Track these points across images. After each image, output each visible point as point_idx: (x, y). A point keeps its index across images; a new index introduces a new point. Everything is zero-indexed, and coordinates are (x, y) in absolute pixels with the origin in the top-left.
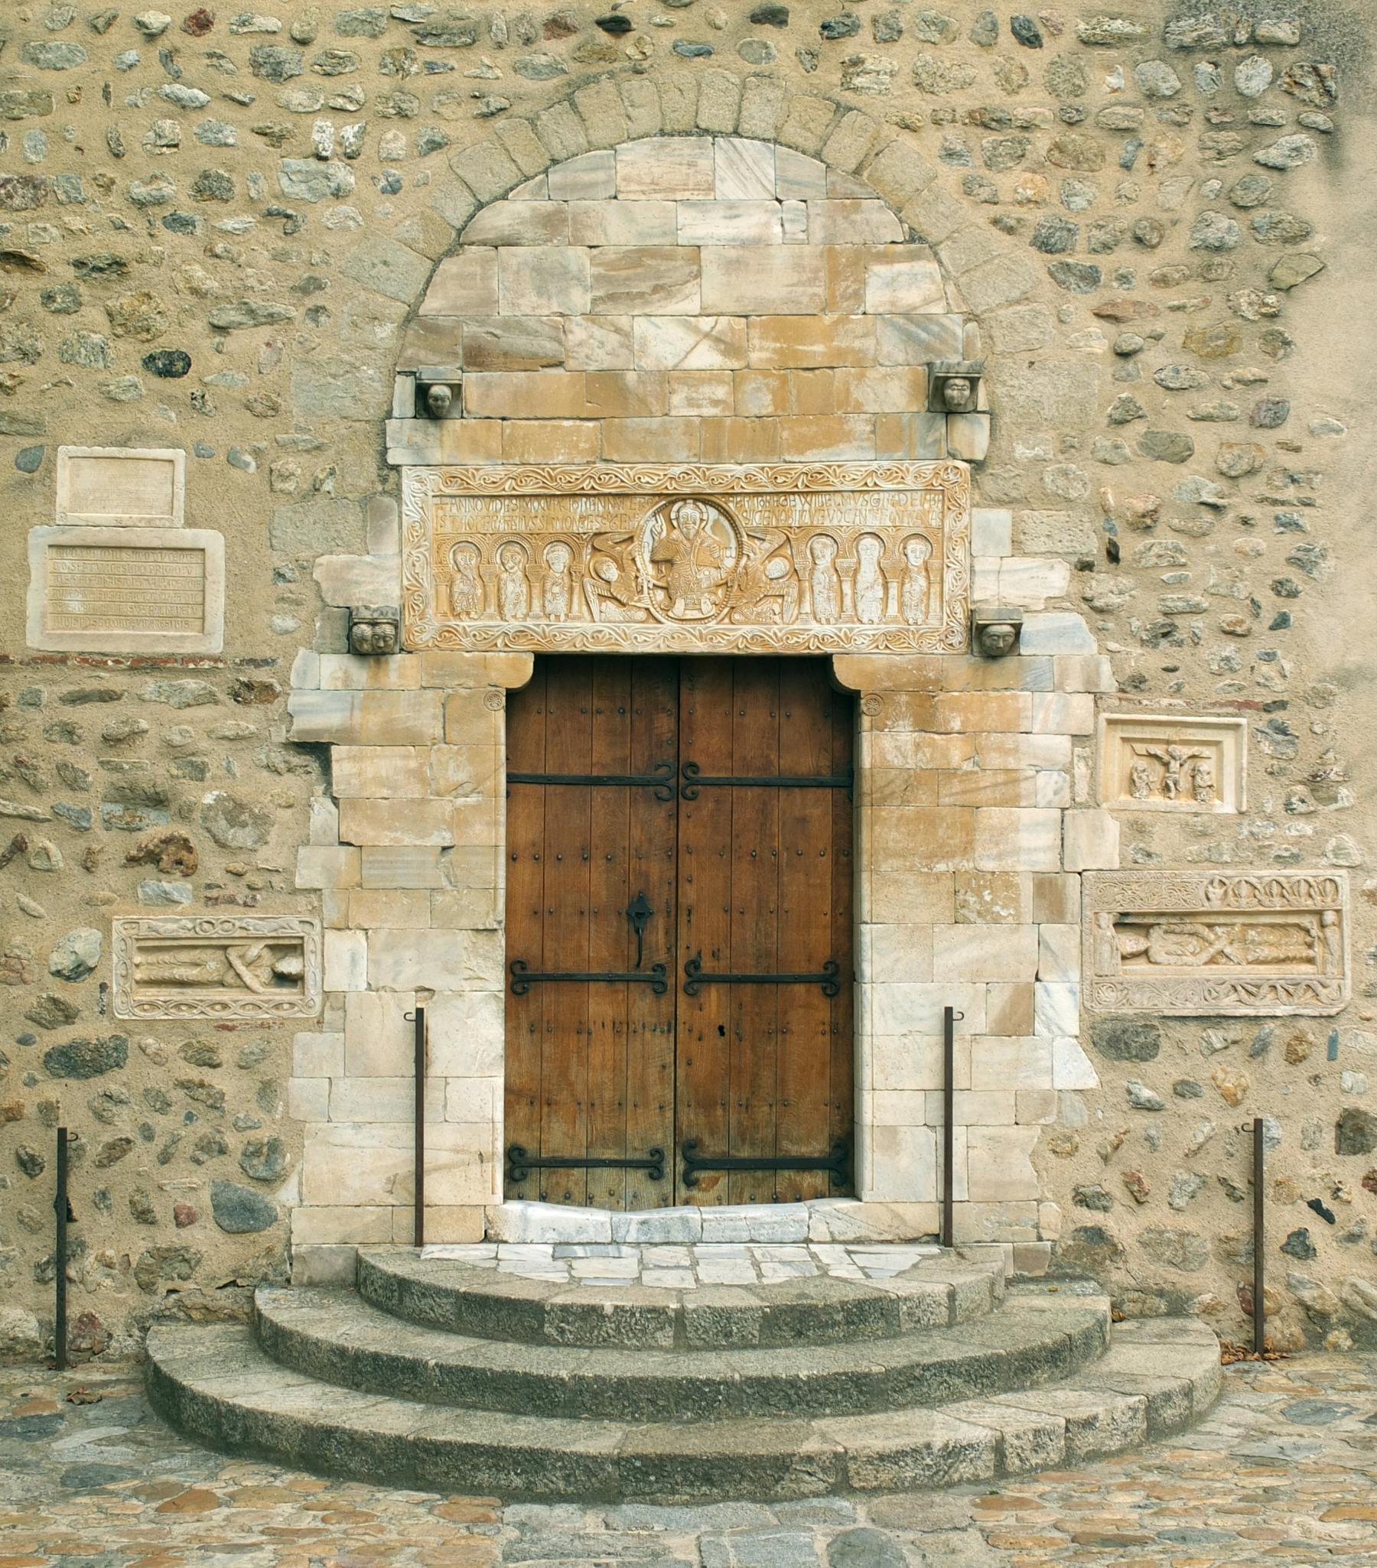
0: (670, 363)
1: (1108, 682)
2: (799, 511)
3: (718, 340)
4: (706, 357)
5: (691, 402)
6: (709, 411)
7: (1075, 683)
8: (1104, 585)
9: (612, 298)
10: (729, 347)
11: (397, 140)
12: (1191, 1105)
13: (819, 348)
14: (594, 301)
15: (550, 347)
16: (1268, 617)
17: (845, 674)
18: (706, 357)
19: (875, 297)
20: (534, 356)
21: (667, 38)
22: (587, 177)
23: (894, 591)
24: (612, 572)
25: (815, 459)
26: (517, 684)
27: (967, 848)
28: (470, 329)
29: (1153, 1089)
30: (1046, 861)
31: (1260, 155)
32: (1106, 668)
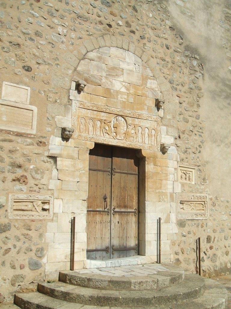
0: (118, 89)
1: (179, 160)
2: (137, 121)
3: (125, 87)
4: (123, 90)
5: (121, 98)
6: (124, 100)
7: (174, 159)
8: (179, 142)
9: (109, 75)
10: (128, 89)
11: (73, 35)
12: (190, 235)
13: (140, 92)
14: (106, 75)
15: (99, 82)
16: (198, 151)
17: (144, 153)
18: (123, 90)
19: (148, 85)
20: (96, 83)
21: (118, 31)
22: (106, 51)
23: (150, 139)
24: (107, 128)
25: (140, 112)
26: (92, 148)
27: (161, 187)
28: (86, 75)
29: (185, 233)
30: (171, 191)
31: (196, 75)
32: (178, 157)
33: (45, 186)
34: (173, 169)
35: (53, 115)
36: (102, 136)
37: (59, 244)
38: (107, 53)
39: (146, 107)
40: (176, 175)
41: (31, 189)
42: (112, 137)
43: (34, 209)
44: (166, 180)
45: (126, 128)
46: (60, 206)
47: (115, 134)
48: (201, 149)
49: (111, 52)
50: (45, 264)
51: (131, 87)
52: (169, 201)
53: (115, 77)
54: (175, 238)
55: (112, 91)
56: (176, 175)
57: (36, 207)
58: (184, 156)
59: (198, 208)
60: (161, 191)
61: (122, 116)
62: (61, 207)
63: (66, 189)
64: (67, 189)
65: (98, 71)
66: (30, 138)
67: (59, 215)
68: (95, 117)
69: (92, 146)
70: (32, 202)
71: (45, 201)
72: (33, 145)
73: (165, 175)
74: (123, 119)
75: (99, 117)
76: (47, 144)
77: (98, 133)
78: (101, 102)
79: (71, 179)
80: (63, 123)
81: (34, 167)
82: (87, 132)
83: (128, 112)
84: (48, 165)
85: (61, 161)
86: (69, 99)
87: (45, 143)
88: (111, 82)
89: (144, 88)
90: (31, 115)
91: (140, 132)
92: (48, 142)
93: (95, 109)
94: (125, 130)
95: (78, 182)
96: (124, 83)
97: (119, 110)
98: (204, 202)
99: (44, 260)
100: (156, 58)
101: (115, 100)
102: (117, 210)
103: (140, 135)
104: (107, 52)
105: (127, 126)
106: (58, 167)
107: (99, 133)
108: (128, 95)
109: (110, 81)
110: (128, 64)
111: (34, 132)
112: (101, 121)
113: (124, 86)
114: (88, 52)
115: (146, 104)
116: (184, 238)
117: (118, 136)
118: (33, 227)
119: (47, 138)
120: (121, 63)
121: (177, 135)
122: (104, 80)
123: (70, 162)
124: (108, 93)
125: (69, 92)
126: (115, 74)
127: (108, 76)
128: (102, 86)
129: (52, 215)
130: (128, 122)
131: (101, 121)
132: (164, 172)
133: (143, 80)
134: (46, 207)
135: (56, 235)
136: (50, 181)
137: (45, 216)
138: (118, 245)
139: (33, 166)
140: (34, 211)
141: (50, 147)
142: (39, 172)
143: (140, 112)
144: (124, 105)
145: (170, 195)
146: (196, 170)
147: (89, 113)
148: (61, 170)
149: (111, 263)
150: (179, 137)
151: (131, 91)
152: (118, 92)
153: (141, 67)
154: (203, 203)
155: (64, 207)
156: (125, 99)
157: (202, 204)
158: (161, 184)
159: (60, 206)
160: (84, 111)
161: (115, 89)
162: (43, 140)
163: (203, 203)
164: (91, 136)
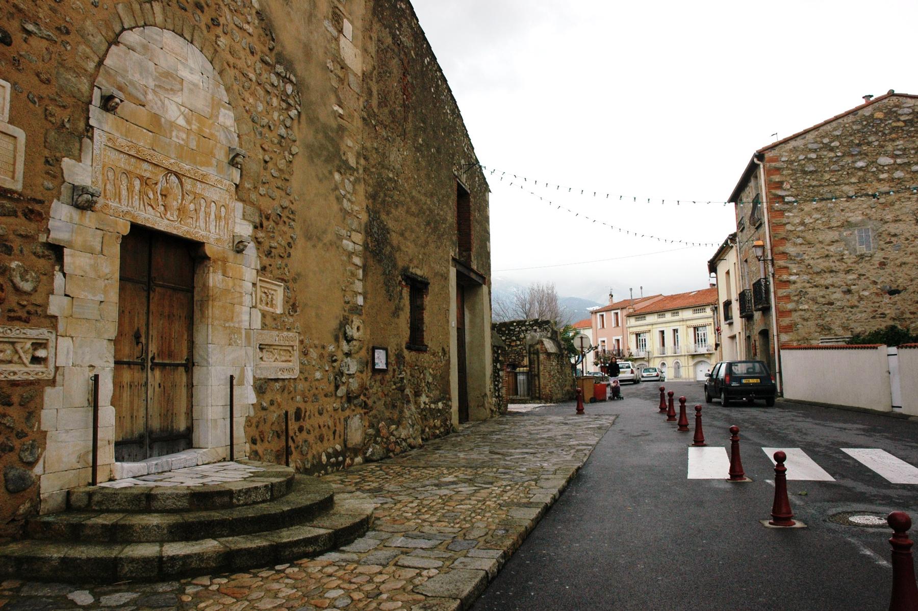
0: (173, 119)
4: (181, 122)
5: (177, 137)
6: (182, 142)
8: (260, 234)
9: (160, 86)
10: (188, 122)
12: (272, 408)
14: (155, 85)
15: (142, 97)
17: (208, 251)
18: (181, 122)
20: (138, 99)
22: (155, 37)
24: (151, 196)
26: (125, 234)
33: (39, 310)
34: (251, 285)
35: (58, 155)
36: (142, 211)
37: (67, 431)
38: (156, 40)
39: (214, 162)
40: (254, 295)
41: (12, 314)
42: (159, 215)
43: (16, 358)
44: (241, 304)
45: (180, 197)
46: (68, 353)
47: (163, 208)
48: (291, 251)
49: (165, 40)
50: (40, 477)
51: (194, 118)
52: (244, 345)
53: (169, 94)
54: (252, 414)
55: (163, 120)
56: (254, 295)
57: (22, 354)
58: (266, 261)
59: (284, 358)
60: (232, 325)
61: (176, 174)
62: (71, 353)
63: (79, 316)
64: (82, 317)
65: (141, 74)
66: (11, 199)
67: (67, 371)
68: (131, 168)
69: (126, 230)
70: (13, 343)
71: (38, 341)
72: (17, 216)
73: (239, 295)
74: (177, 181)
75: (138, 172)
76: (44, 216)
77: (136, 204)
78: (144, 141)
79: (90, 297)
80: (77, 174)
81: (18, 266)
82: (117, 200)
83: (188, 167)
84: (42, 263)
85: (72, 255)
86: (87, 124)
87: (40, 214)
88: (163, 103)
89: (213, 124)
90: (11, 147)
91: (203, 209)
92: (48, 213)
93: (132, 153)
94: (180, 201)
95: (101, 302)
96: (183, 109)
97: (172, 161)
98: (292, 346)
99: (38, 469)
100: (234, 67)
101: (168, 140)
102: (156, 361)
103: (202, 215)
104: (158, 38)
105: (183, 195)
106: (67, 269)
107: (138, 202)
108: (189, 131)
109: (161, 100)
110: (192, 71)
111: (18, 187)
112: (141, 178)
113: (182, 113)
114: (124, 29)
115: (215, 155)
116: (263, 413)
117: (169, 213)
118: (15, 399)
119: (46, 202)
120: (180, 67)
121: (257, 220)
122: (150, 96)
123: (88, 261)
124: (157, 124)
125: (88, 110)
126: (168, 87)
127: (157, 89)
128: (147, 107)
129: (53, 370)
130: (185, 188)
131: (141, 178)
132: (238, 289)
133: (213, 108)
134: (41, 353)
135: (62, 412)
136: (51, 297)
137: (40, 374)
138: (162, 430)
139: (16, 262)
140: (16, 363)
141: (51, 223)
142: (28, 277)
143: (204, 170)
144: (182, 152)
145: (246, 333)
146: (282, 288)
147: (123, 162)
148: (71, 276)
149: (156, 464)
150: (262, 226)
151: (194, 127)
152: (173, 125)
153: (211, 81)
154: (290, 349)
155: (75, 353)
156: (183, 140)
157: (288, 350)
158: (233, 313)
159: (68, 353)
160: (114, 155)
161: (167, 117)
162: (37, 207)
163: (290, 349)
164: (125, 208)
